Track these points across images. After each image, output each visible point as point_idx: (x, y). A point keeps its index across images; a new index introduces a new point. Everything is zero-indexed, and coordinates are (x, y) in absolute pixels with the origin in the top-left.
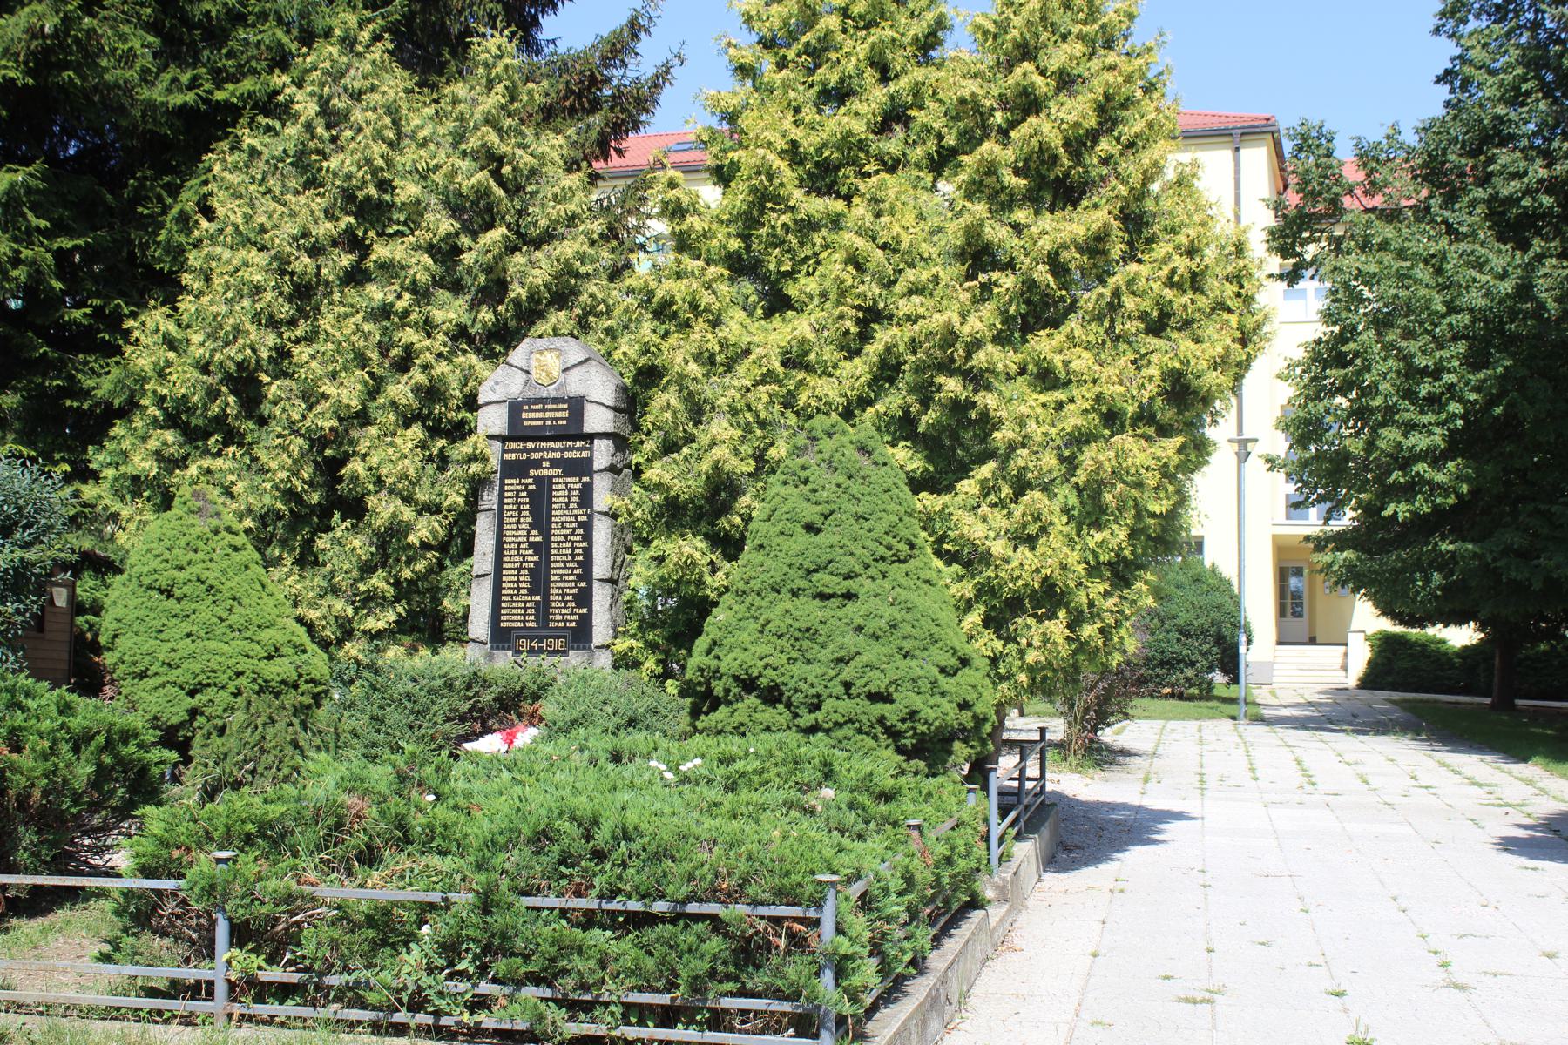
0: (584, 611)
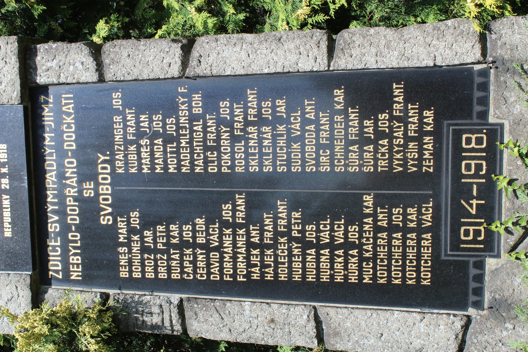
0: (398, 91)
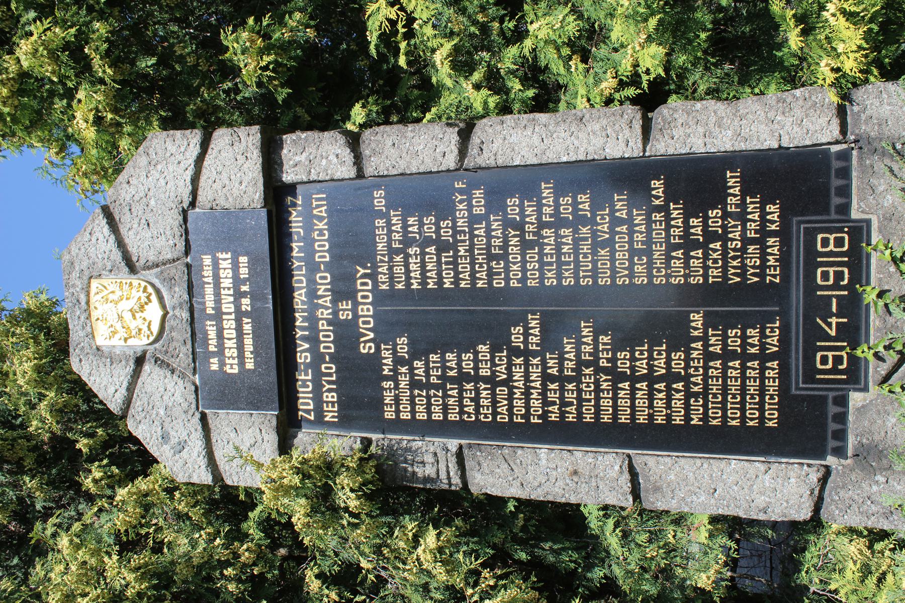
0: (733, 180)
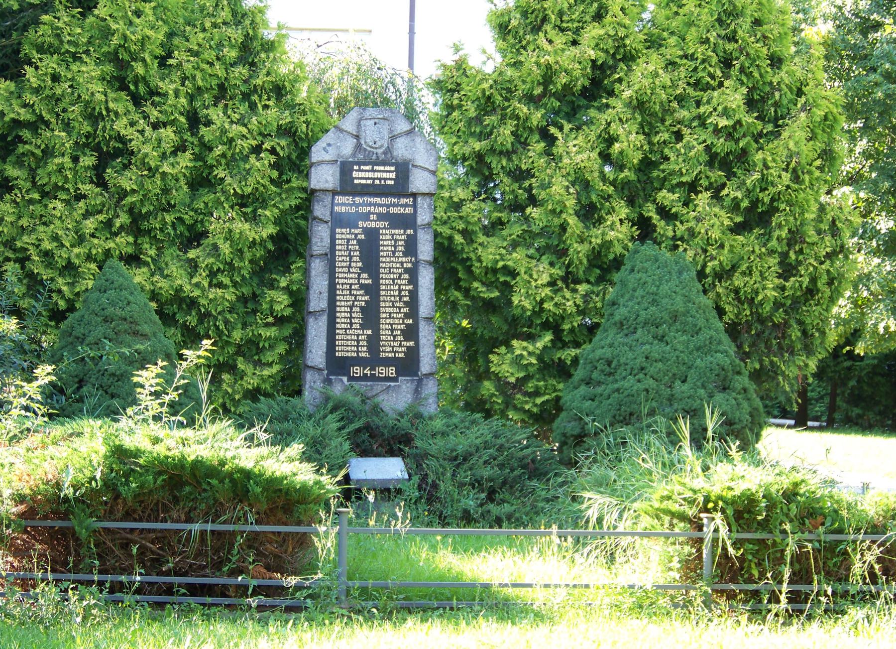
0: (411, 344)
